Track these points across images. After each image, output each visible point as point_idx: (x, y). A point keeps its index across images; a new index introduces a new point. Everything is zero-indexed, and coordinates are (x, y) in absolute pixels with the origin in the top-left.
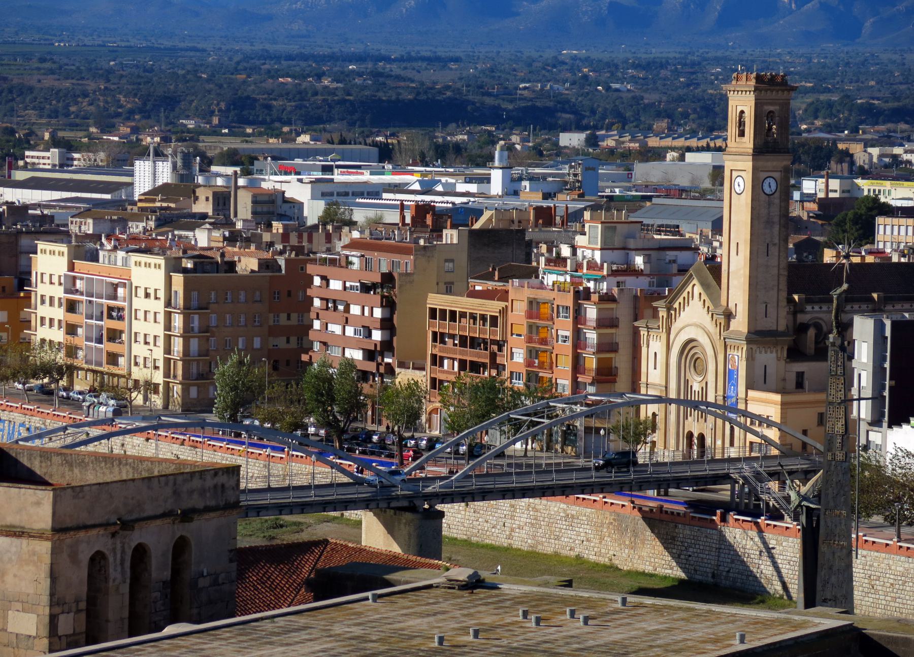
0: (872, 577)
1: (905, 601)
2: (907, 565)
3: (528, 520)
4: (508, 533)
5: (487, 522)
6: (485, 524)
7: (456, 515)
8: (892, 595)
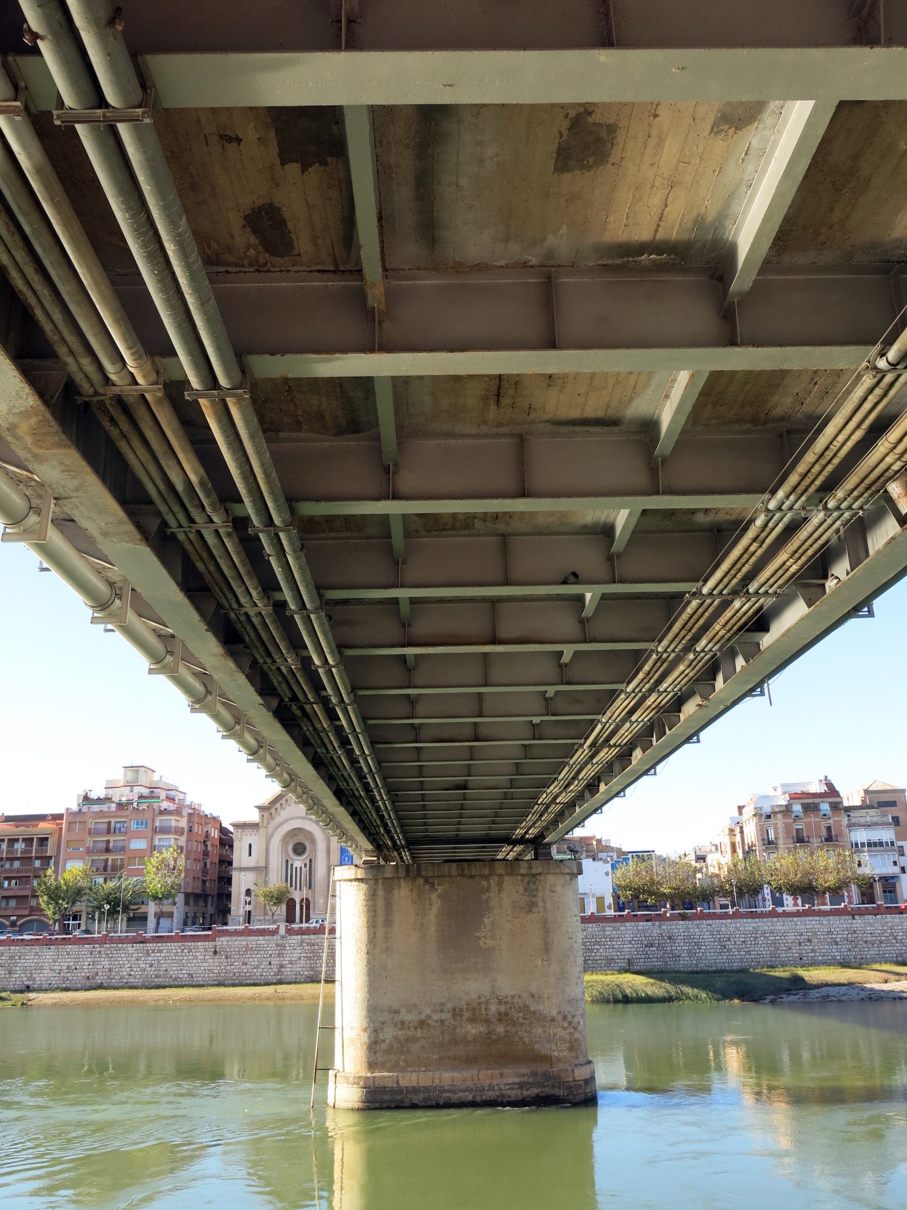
0: (722, 940)
1: (759, 953)
2: (754, 925)
3: (302, 955)
4: (276, 970)
5: (246, 964)
6: (244, 967)
7: (201, 964)
8: (745, 950)
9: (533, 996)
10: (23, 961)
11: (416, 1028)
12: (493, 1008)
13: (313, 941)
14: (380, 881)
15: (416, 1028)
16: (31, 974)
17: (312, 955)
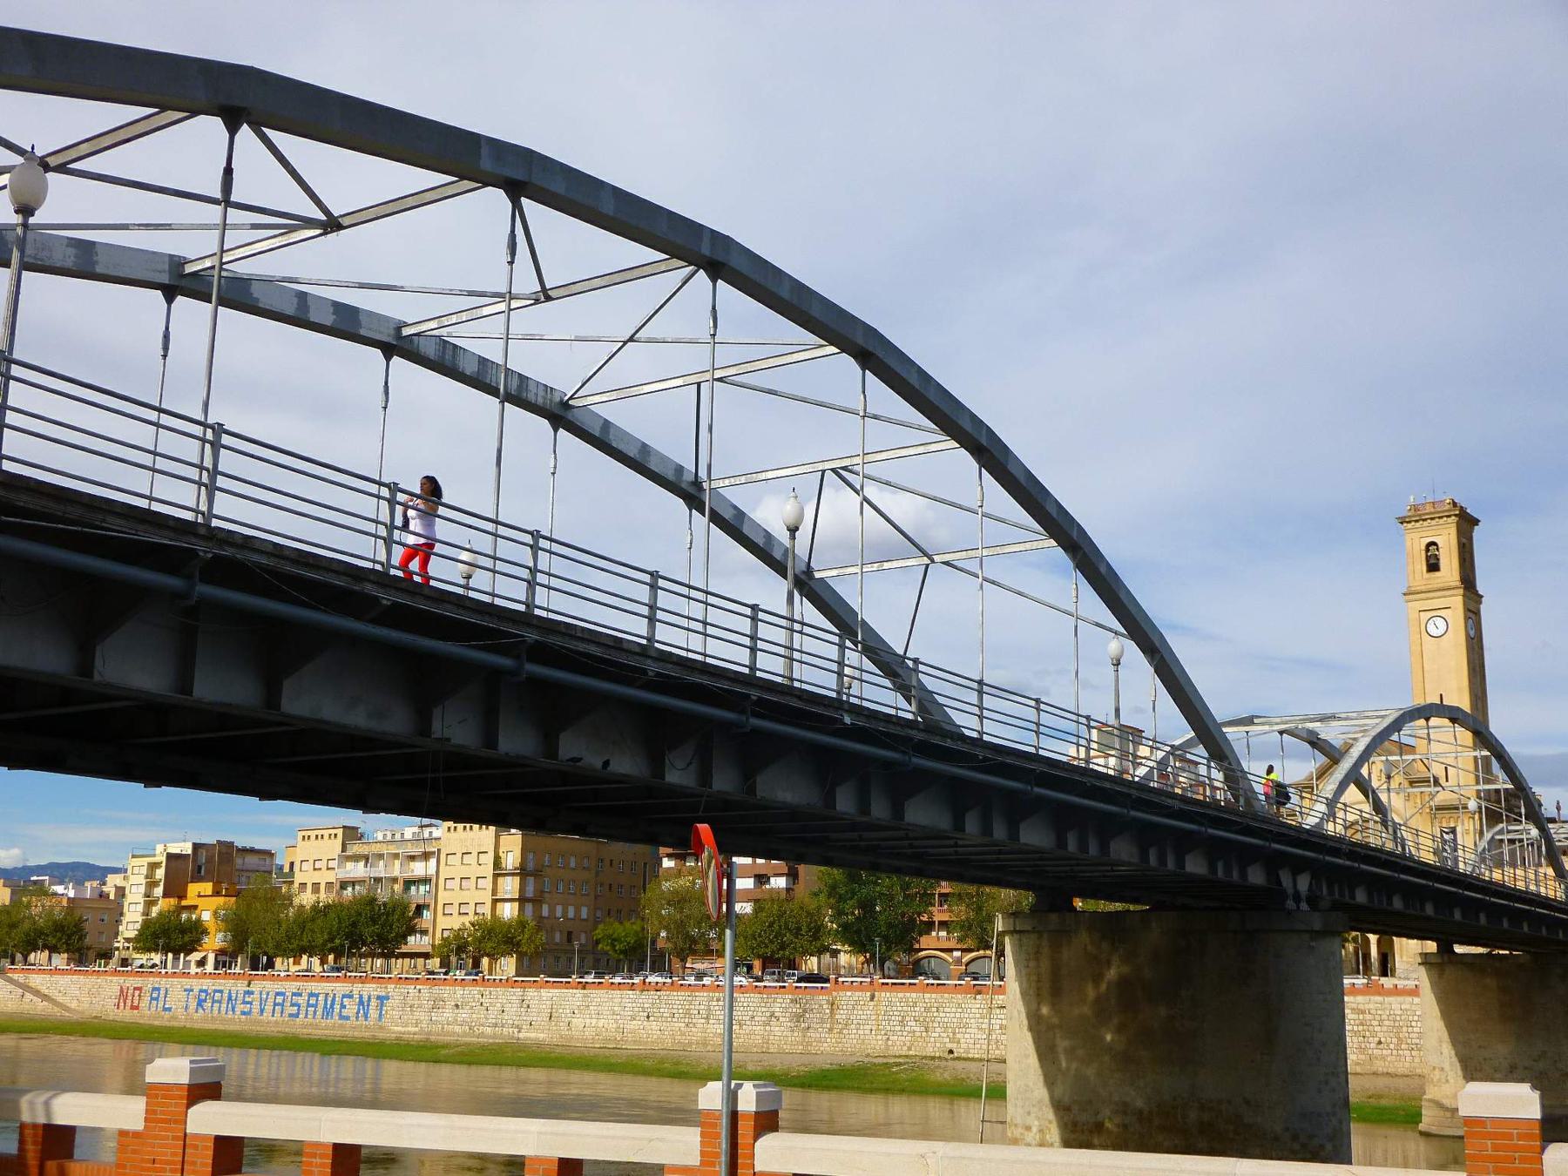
9: (1247, 1102)
10: (941, 1015)
11: (1091, 1132)
12: (1193, 1115)
13: (1361, 1007)
14: (1045, 935)
15: (1091, 1132)
16: (954, 1033)
17: (1361, 1028)
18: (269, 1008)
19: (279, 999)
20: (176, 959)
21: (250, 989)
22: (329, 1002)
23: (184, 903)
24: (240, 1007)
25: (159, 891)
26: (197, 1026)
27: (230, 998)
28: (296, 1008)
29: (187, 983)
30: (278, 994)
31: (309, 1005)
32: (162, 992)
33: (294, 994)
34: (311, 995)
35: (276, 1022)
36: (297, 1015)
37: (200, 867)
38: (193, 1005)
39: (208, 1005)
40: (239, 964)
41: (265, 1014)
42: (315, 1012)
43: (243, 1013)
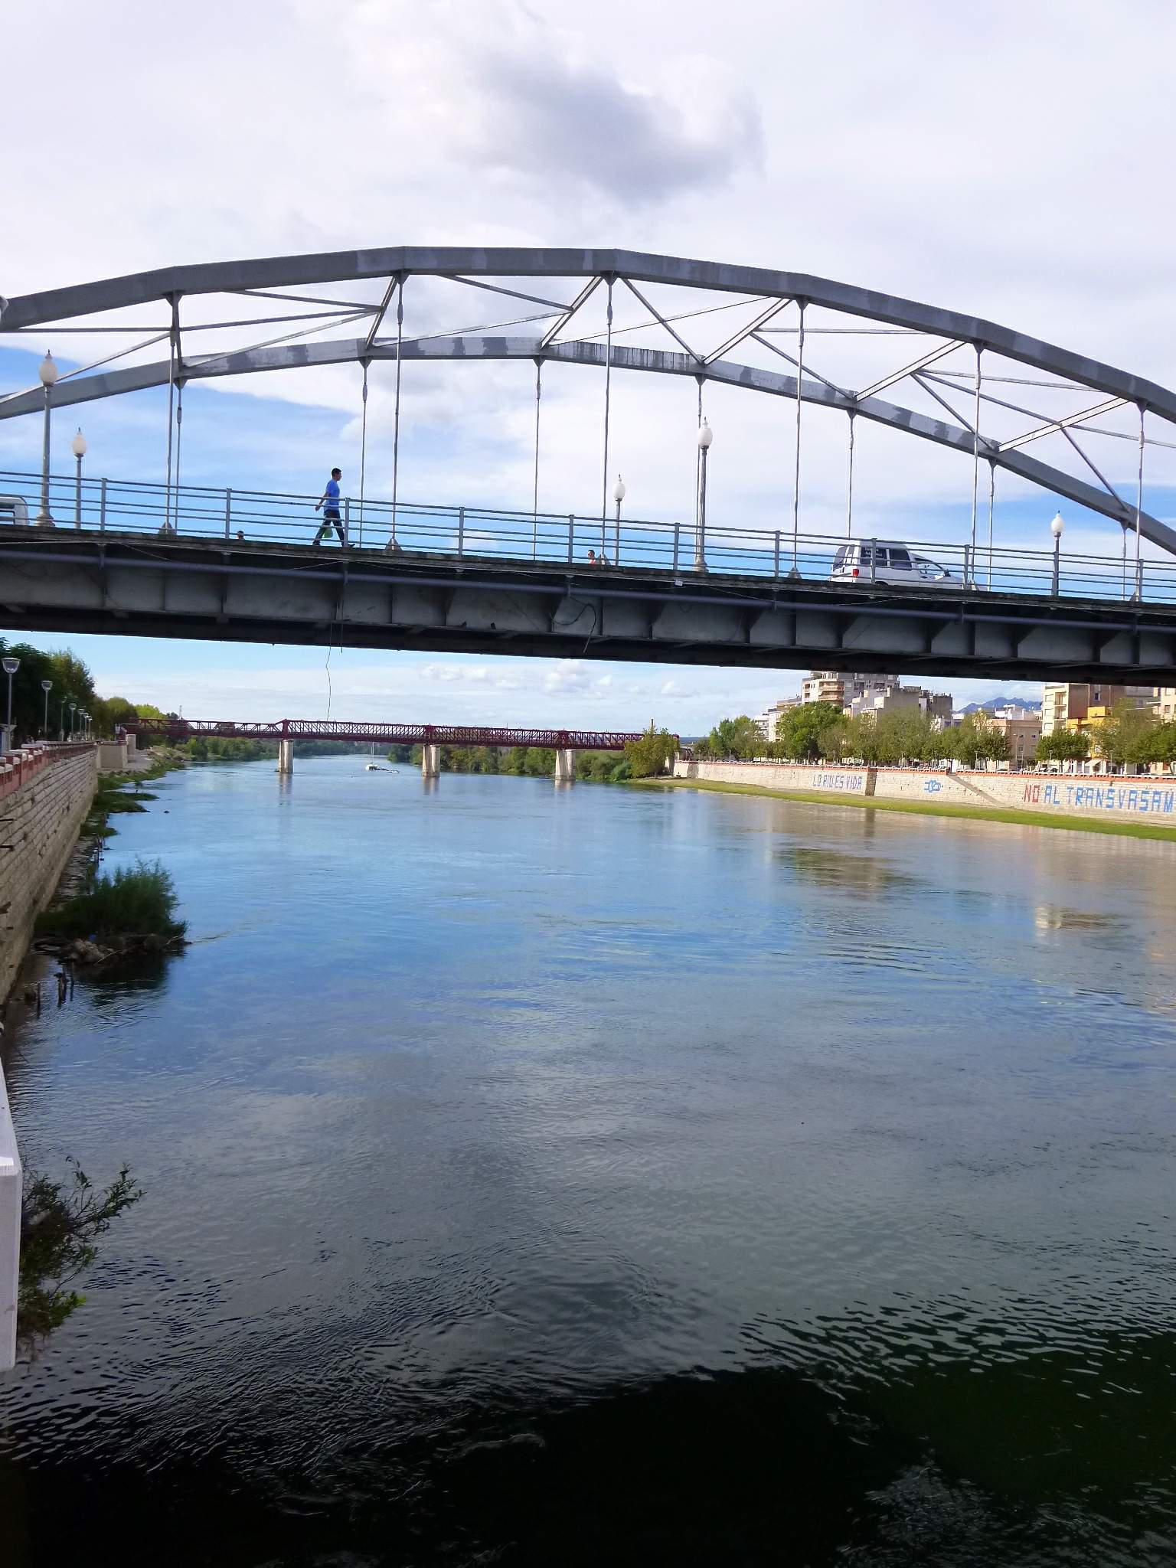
18: (1126, 803)
19: (1133, 796)
20: (1079, 765)
21: (1112, 788)
22: (1169, 799)
23: (1083, 722)
24: (1105, 802)
25: (1065, 714)
26: (1077, 815)
27: (1098, 795)
28: (1145, 803)
29: (1070, 782)
30: (1132, 792)
31: (1154, 801)
32: (1053, 789)
33: (1143, 792)
34: (1156, 793)
35: (1131, 813)
36: (1145, 809)
37: (1097, 694)
38: (1073, 799)
39: (1083, 800)
40: (1125, 769)
41: (1123, 807)
42: (1159, 806)
43: (1108, 806)
